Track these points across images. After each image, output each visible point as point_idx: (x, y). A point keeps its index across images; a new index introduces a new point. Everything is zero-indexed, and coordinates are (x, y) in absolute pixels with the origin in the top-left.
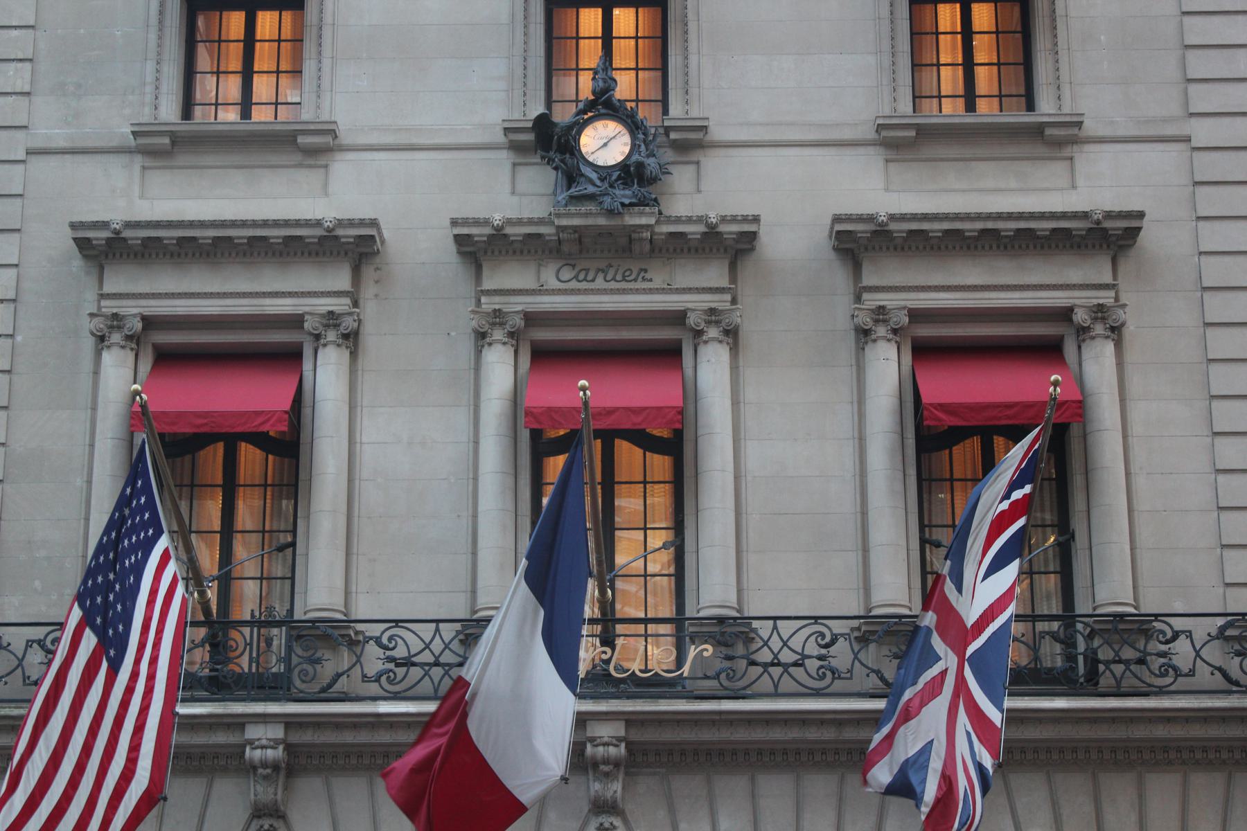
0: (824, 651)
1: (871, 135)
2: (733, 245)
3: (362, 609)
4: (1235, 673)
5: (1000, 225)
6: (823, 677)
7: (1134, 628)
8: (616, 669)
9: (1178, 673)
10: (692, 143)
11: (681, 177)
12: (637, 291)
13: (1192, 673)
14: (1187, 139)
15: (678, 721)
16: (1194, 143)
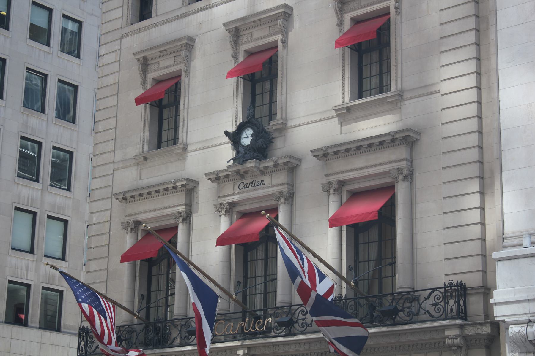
0: (304, 317)
1: (334, 113)
2: (292, 166)
3: (418, 287)
4: (433, 313)
5: (373, 141)
6: (303, 327)
7: (412, 297)
8: (260, 329)
9: (414, 315)
10: (283, 128)
11: (278, 143)
12: (260, 189)
13: (418, 314)
14: (439, 92)
15: (400, 334)
16: (442, 93)
